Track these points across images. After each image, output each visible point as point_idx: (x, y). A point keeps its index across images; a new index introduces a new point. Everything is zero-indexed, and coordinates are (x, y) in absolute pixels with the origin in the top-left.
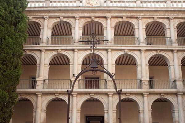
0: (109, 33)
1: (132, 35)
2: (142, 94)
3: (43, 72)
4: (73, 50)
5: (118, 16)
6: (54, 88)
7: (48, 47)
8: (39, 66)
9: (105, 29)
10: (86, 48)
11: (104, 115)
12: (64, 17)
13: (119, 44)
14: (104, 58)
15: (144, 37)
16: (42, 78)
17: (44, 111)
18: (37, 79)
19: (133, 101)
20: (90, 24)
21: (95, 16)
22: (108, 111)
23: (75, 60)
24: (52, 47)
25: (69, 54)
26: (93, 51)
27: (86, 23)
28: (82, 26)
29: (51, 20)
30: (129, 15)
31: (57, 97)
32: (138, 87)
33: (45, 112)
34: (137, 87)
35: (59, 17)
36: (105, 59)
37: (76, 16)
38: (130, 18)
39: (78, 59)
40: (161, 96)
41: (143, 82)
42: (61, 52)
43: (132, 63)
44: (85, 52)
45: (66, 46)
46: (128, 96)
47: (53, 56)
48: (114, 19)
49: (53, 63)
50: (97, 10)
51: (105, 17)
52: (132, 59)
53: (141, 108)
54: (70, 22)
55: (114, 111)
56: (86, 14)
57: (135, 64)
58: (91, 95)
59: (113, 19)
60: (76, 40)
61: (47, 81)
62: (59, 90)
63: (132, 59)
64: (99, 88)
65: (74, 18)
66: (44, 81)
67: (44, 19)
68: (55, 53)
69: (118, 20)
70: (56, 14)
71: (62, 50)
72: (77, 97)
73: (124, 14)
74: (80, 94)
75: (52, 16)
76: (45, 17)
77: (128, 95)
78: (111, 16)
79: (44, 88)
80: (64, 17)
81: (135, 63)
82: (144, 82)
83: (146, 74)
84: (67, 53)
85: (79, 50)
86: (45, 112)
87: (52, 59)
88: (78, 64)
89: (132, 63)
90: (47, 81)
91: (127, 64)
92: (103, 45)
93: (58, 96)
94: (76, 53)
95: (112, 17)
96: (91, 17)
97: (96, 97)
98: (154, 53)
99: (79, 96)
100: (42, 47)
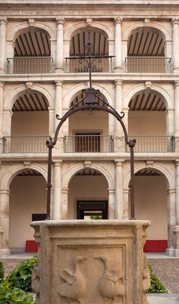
0: (119, 51)
1: (161, 55)
4: (54, 83)
5: (136, 17)
6: (22, 151)
7: (9, 77)
9: (112, 43)
10: (77, 79)
11: (108, 198)
12: (36, 20)
13: (136, 72)
17: (6, 192)
19: (158, 175)
20: (84, 33)
21: (93, 17)
22: (114, 190)
23: (57, 103)
24: (16, 77)
25: (47, 91)
26: (89, 84)
27: (76, 31)
28: (68, 38)
29: (11, 24)
30: (155, 14)
31: (27, 167)
32: (168, 149)
34: (166, 151)
35: (27, 20)
36: (110, 99)
37: (57, 18)
38: (159, 20)
39: (63, 99)
42: (31, 86)
43: (159, 106)
44: (75, 86)
45: (41, 76)
47: (18, 94)
48: (128, 23)
49: (18, 108)
50: (98, 5)
51: (112, 20)
52: (160, 99)
54: (47, 29)
55: (125, 192)
56: (76, 13)
57: (165, 109)
58: (85, 163)
59: (125, 24)
60: (58, 64)
61: (9, 140)
62: (30, 155)
63: (160, 99)
64: (99, 151)
65: (54, 20)
68: (21, 88)
70: (21, 13)
71: (34, 82)
72: (61, 166)
73: (146, 13)
74: (67, 161)
75: (14, 17)
78: (122, 17)
79: (3, 152)
80: (36, 20)
81: (163, 107)
84: (42, 89)
85: (65, 82)
87: (17, 101)
88: (63, 109)
89: (159, 106)
90: (9, 140)
91: (149, 110)
92: (107, 73)
93: (29, 165)
94: (59, 88)
95: (124, 20)
96: (85, 20)
97: (95, 167)
99: (66, 166)
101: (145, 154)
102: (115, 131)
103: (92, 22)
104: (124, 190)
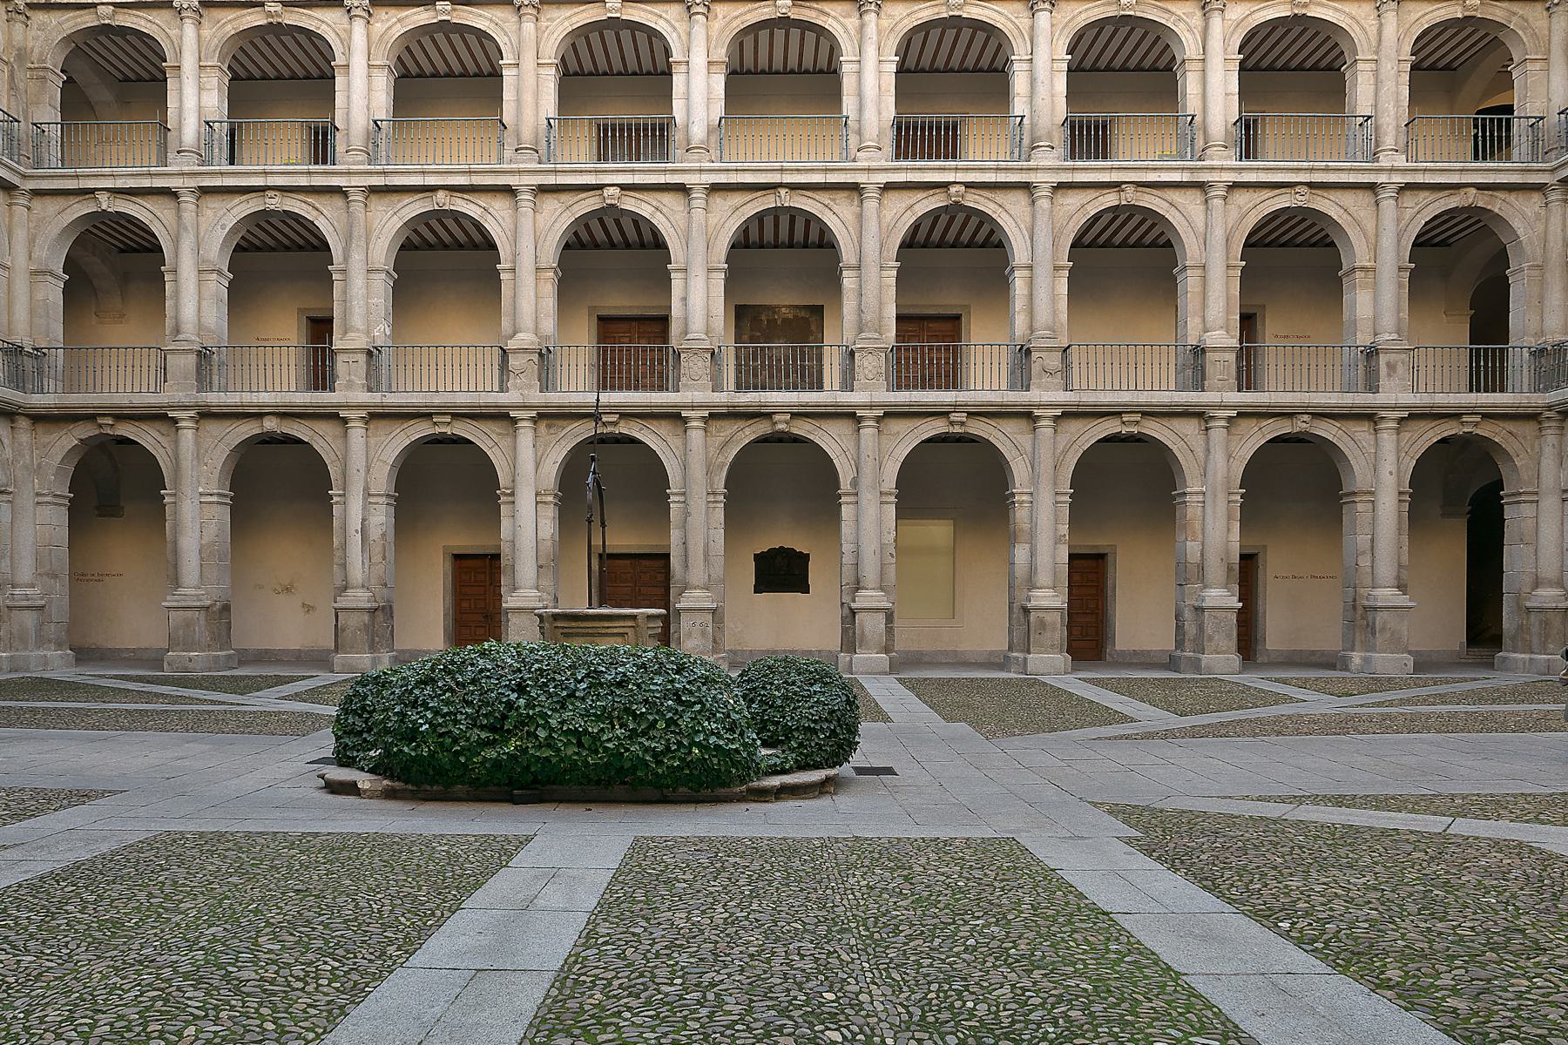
40: (952, 423)
41: (1035, 355)
55: (885, 499)
82: (1042, 354)
93: (615, 424)
98: (1110, 199)
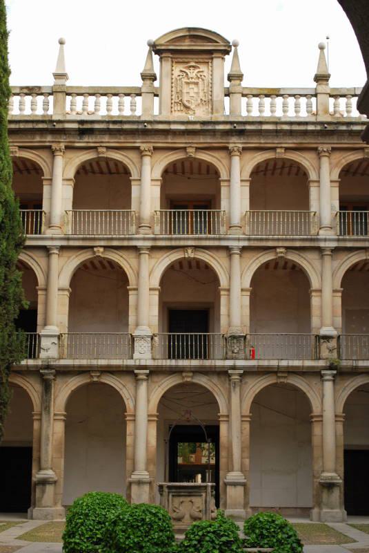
2: (315, 373)
3: (56, 315)
8: (44, 293)
9: (226, 184)
10: (174, 243)
14: (221, 270)
15: (332, 208)
16: (53, 329)
17: (63, 418)
18: (41, 331)
22: (228, 416)
33: (64, 420)
37: (143, 146)
44: (168, 254)
46: (282, 377)
53: (316, 410)
54: (126, 161)
58: (184, 374)
60: (143, 219)
61: (65, 337)
66: (59, 337)
67: (53, 152)
69: (260, 157)
76: (54, 146)
77: (283, 375)
78: (241, 146)
83: (334, 315)
86: (64, 420)
90: (65, 337)
95: (244, 149)
99: (155, 378)
100: (52, 239)
101: (274, 363)
102: (229, 325)
103: (196, 152)
104: (242, 416)
